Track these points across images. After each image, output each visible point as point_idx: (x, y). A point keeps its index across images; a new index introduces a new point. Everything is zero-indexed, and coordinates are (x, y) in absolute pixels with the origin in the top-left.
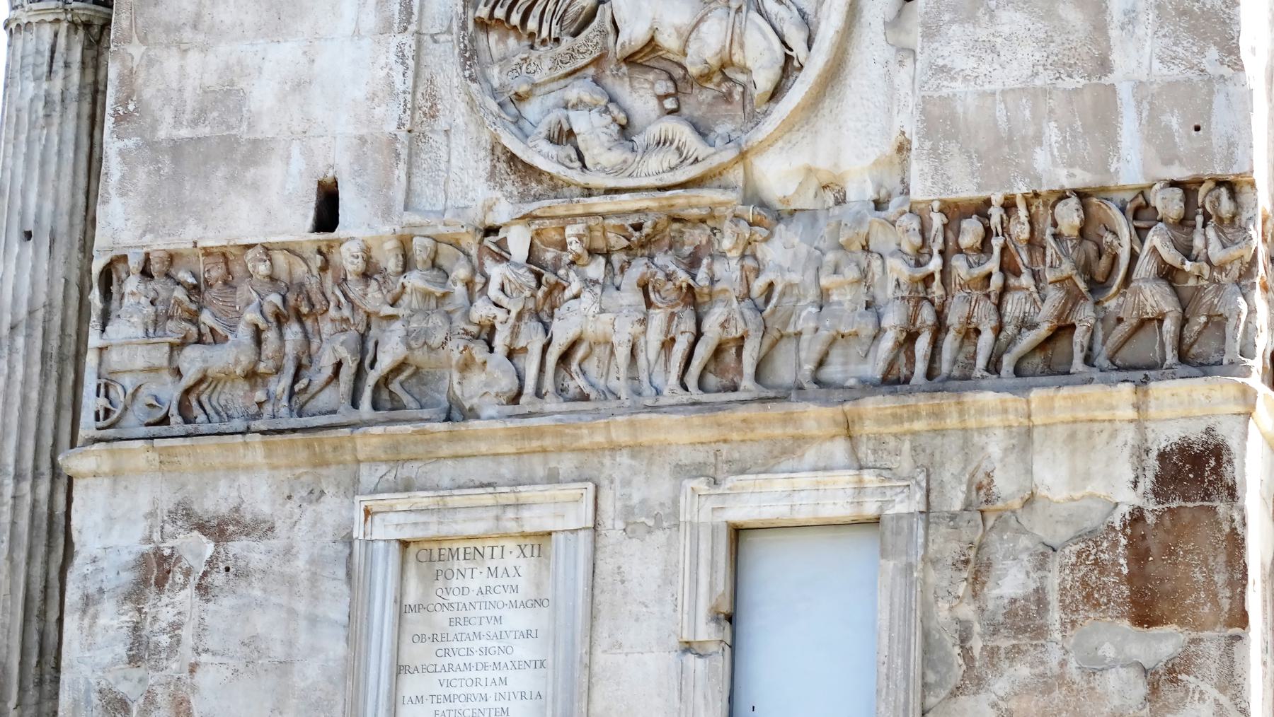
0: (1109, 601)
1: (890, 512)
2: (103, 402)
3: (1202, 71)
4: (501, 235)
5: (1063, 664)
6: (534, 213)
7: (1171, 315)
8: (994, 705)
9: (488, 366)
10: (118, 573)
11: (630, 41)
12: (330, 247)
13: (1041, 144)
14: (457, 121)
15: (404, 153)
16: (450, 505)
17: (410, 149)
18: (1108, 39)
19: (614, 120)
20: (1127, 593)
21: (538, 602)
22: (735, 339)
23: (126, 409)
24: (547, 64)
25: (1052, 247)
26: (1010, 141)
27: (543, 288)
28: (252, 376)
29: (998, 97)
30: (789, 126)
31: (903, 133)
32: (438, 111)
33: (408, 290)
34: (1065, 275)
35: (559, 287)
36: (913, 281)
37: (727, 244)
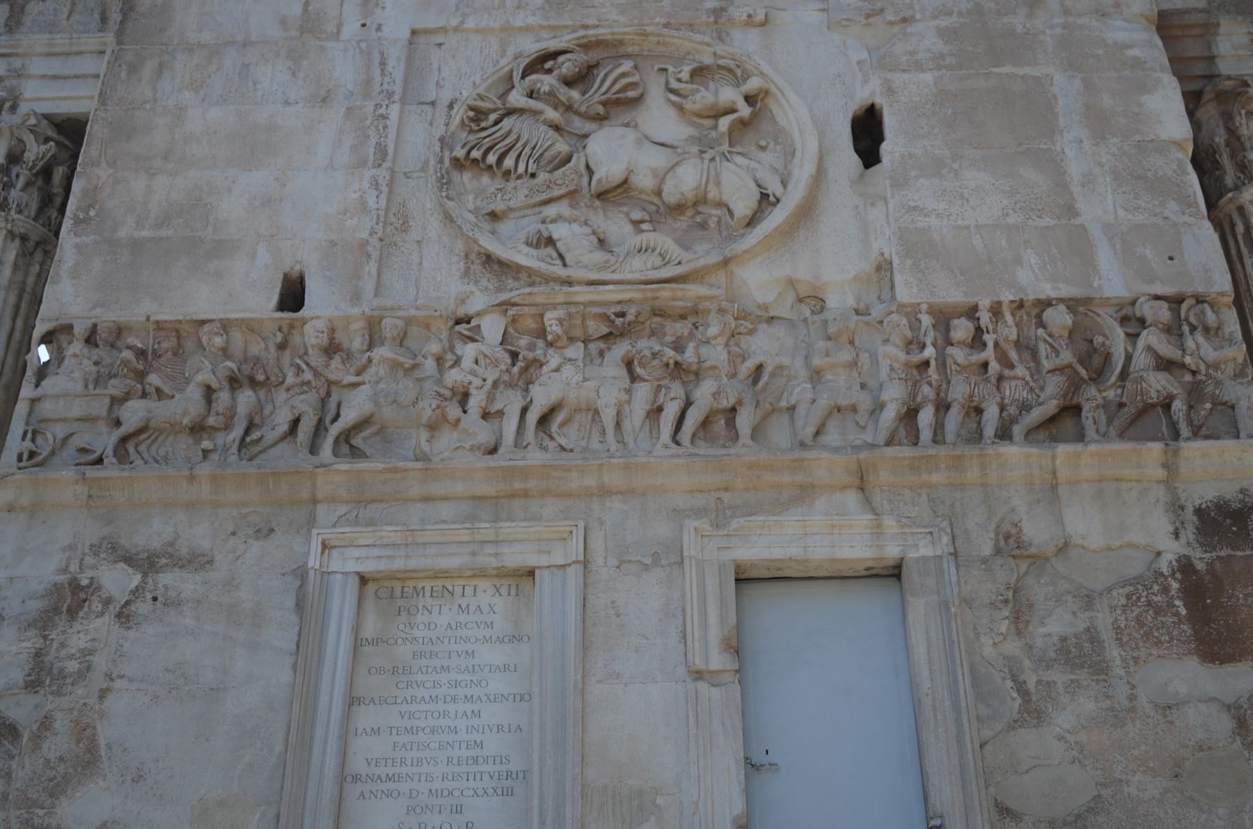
0: (1172, 639)
1: (913, 555)
2: (28, 444)
3: (1166, 218)
4: (473, 323)
5: (1132, 698)
6: (513, 300)
7: (1180, 396)
8: (1060, 738)
9: (462, 425)
10: (24, 602)
12: (292, 327)
13: (1021, 264)
14: (430, 234)
16: (420, 540)
17: (381, 254)
18: (1072, 194)
19: (594, 233)
20: (1189, 632)
21: (516, 638)
22: (724, 411)
23: (53, 453)
25: (1045, 341)
27: (520, 364)
28: (198, 429)
29: (972, 229)
30: (767, 243)
31: (882, 254)
32: (410, 227)
33: (375, 361)
34: (1065, 362)
35: (538, 363)
36: (907, 365)
37: (713, 331)
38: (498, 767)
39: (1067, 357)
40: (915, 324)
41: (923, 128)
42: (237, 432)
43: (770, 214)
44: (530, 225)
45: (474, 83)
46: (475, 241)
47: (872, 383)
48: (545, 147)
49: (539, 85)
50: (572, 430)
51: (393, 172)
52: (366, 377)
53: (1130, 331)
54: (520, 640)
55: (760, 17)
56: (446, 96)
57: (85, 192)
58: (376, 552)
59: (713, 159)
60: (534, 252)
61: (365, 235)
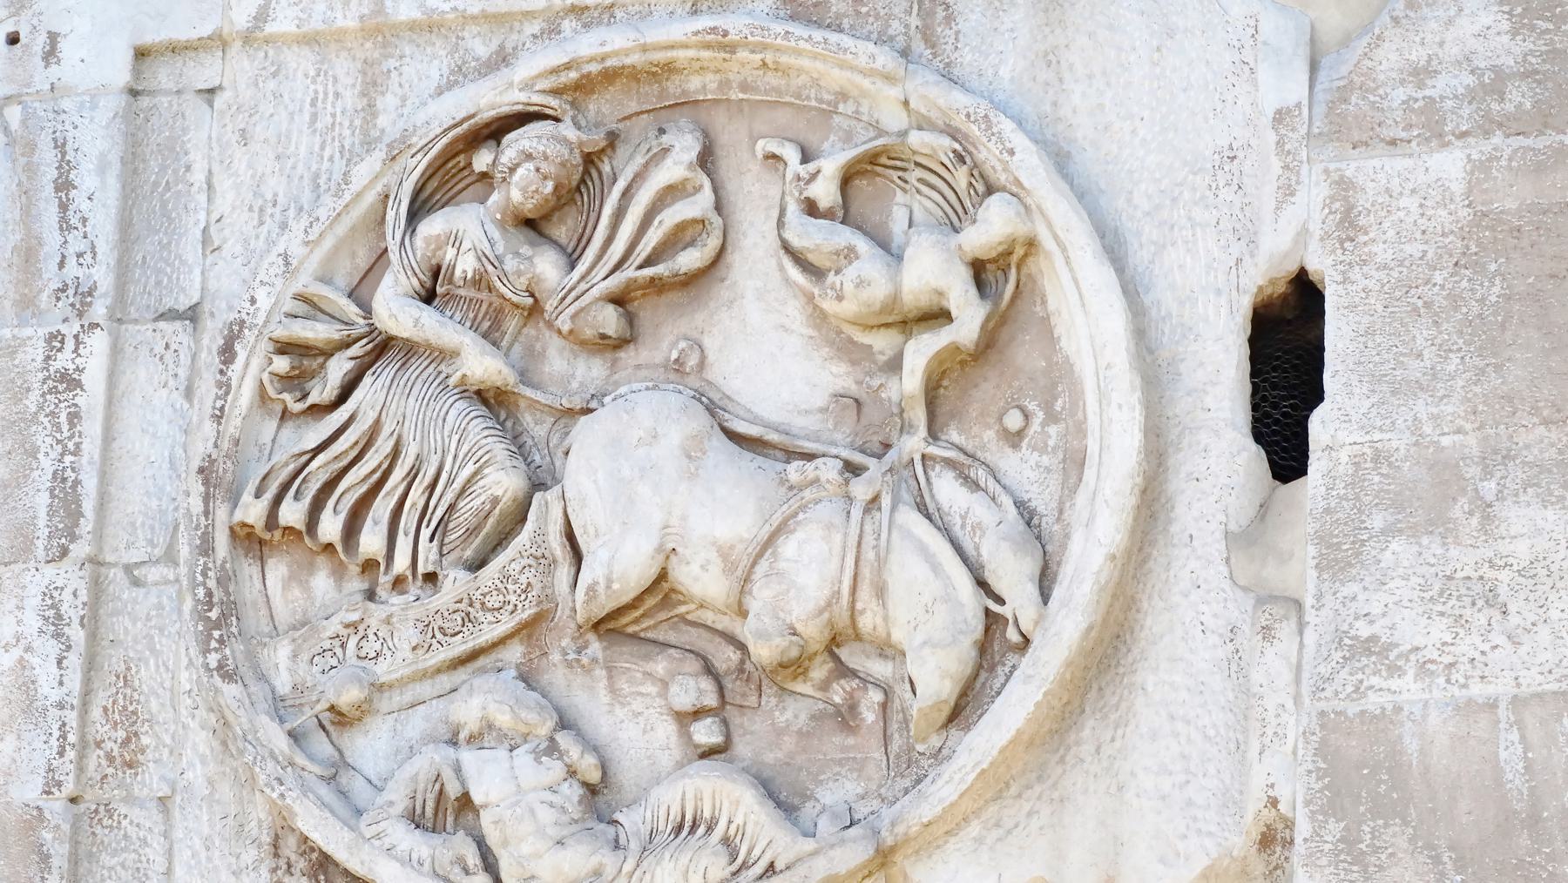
11: (609, 582)
14: (190, 775)
17: (75, 843)
19: (572, 773)
24: (408, 635)
26: (1534, 821)
29: (1502, 712)
31: (1274, 802)
41: (1420, 356)
43: (1008, 678)
45: (285, 257)
48: (457, 485)
49: (450, 253)
59: (874, 502)
61: (29, 791)
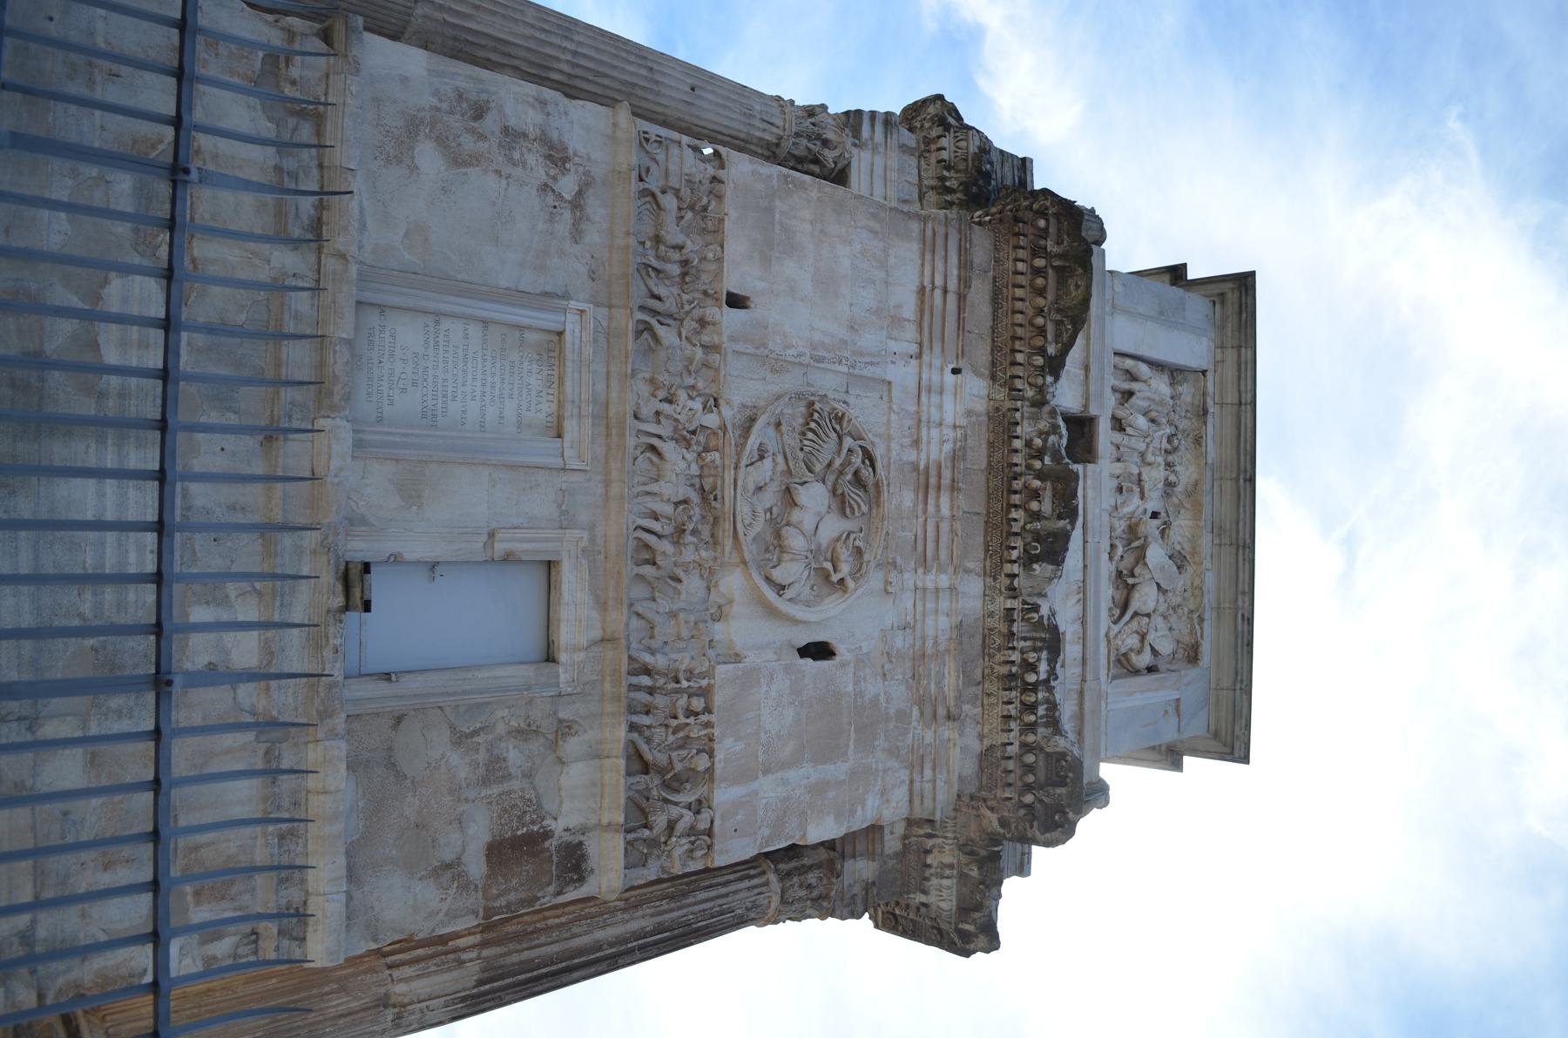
0: (502, 825)
5: (466, 800)
9: (653, 399)
12: (717, 300)
13: (736, 741)
15: (758, 352)
18: (777, 771)
20: (507, 836)
21: (519, 425)
23: (647, 152)
27: (688, 435)
28: (657, 240)
34: (675, 766)
36: (677, 671)
37: (703, 554)
38: (440, 410)
39: (678, 767)
40: (702, 676)
42: (655, 263)
44: (772, 446)
46: (764, 413)
47: (667, 649)
50: (646, 465)
51: (808, 365)
52: (684, 342)
53: (693, 805)
54: (518, 427)
55: (890, 589)
56: (851, 400)
57: (803, 182)
58: (577, 342)
59: (807, 558)
60: (756, 448)
61: (770, 346)
